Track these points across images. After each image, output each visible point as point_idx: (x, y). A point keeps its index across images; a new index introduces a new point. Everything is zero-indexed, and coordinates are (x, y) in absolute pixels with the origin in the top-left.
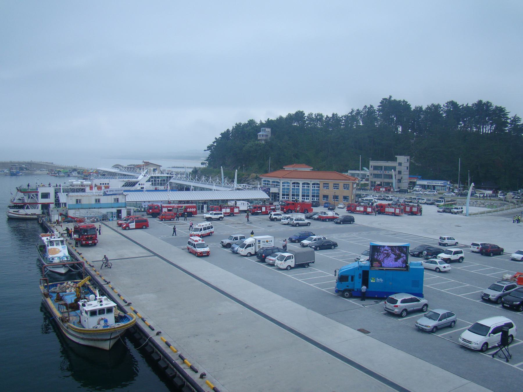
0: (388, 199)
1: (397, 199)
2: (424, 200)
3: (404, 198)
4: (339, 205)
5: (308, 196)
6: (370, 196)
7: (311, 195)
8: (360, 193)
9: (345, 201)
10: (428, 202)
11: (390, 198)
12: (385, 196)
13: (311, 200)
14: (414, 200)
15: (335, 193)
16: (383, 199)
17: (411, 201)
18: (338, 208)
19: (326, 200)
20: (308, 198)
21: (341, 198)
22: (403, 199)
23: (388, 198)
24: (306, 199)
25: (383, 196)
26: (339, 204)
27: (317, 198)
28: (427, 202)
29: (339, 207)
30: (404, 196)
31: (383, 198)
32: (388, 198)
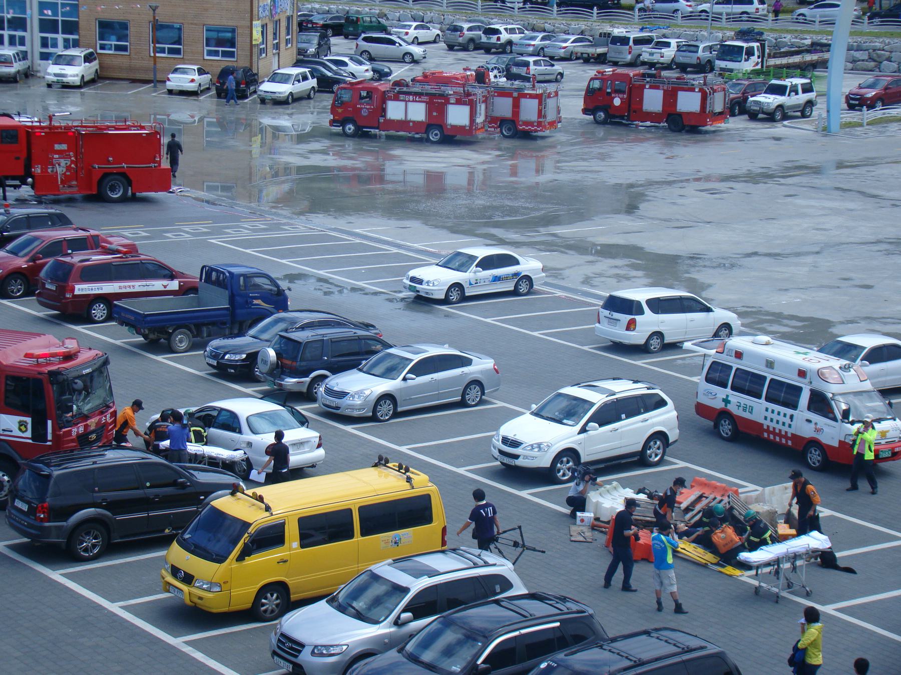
0: (494, 45)
1: (536, 42)
2: (668, 45)
3: (573, 38)
4: (171, 76)
5: (19, 24)
6: (404, 27)
7: (33, 16)
8: (367, 9)
9: (216, 53)
10: (691, 59)
11: (503, 41)
12: (478, 28)
13: (38, 49)
14: (618, 46)
15: (154, 9)
16: (471, 47)
17: (606, 54)
18: (170, 92)
19: (118, 48)
20: (19, 33)
21: (195, 37)
22: (565, 41)
23: (493, 39)
24: (12, 41)
25: (470, 29)
26: (176, 71)
27: (71, 37)
28: (677, 60)
29: (170, 85)
30: (582, 25)
31: (472, 40)
32: (493, 39)
